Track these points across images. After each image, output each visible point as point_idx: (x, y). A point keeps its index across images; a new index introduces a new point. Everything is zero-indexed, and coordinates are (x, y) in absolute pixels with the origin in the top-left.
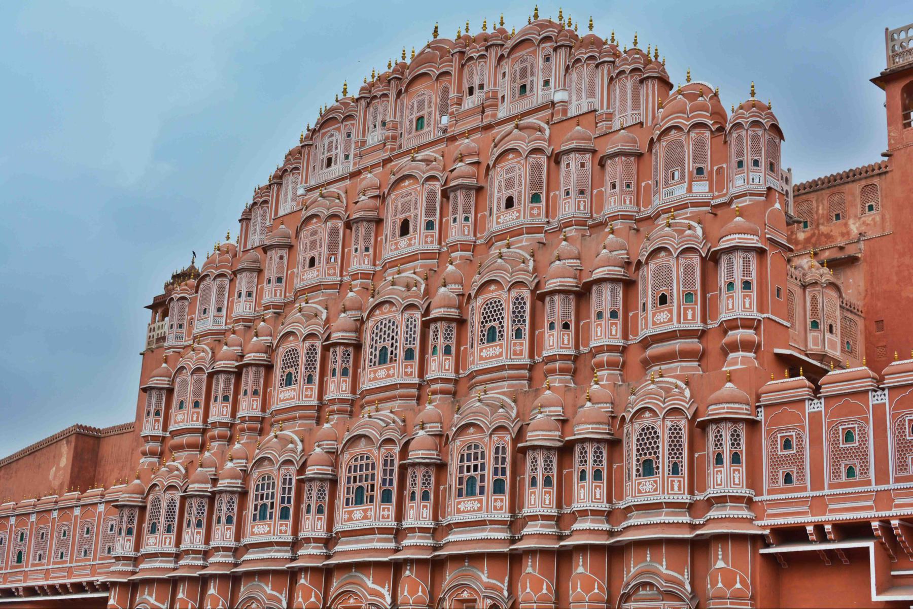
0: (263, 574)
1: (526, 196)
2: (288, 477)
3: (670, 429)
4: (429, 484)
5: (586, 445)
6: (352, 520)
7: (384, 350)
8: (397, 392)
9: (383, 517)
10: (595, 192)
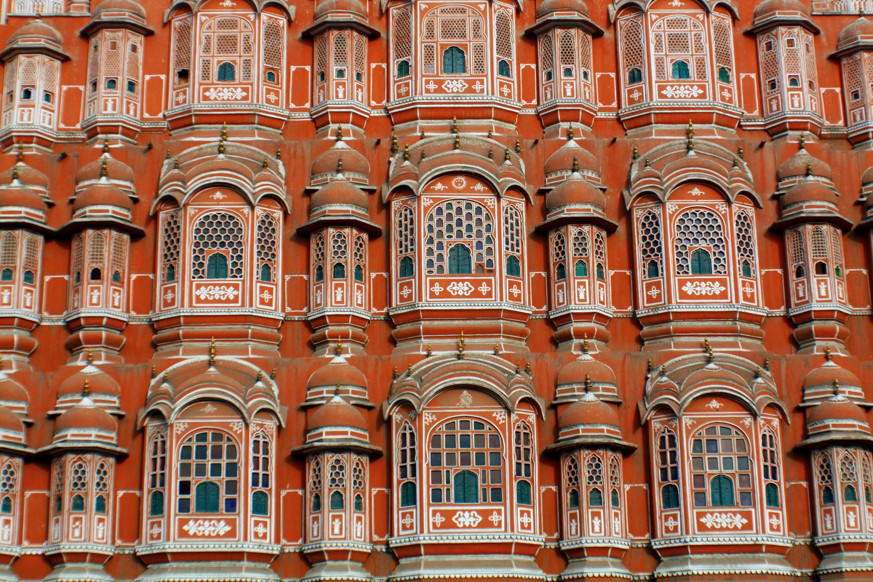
1: (711, 69)
2: (261, 440)
6: (455, 526)
8: (501, 323)
9: (523, 527)
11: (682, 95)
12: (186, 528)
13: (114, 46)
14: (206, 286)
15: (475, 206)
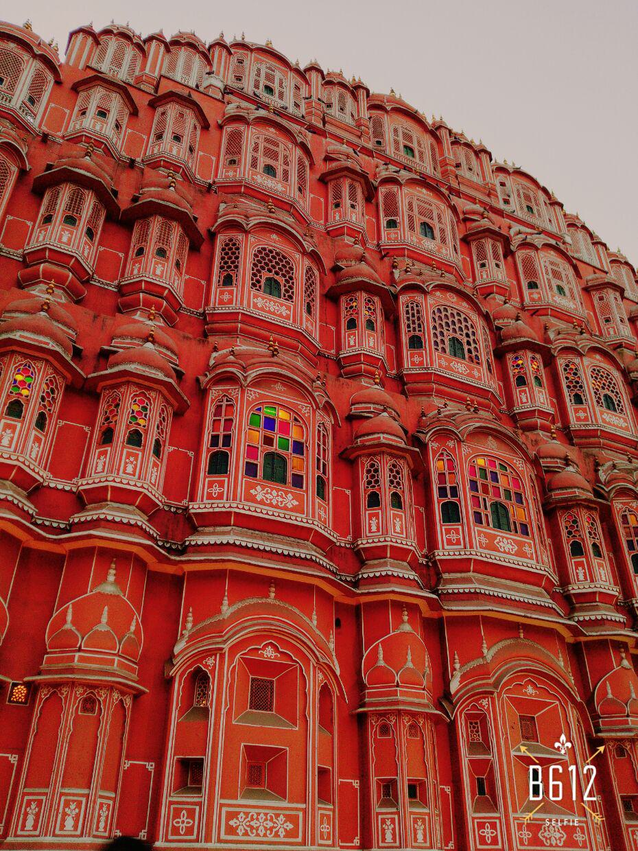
0: (288, 589)
7: (455, 341)
11: (565, 303)
12: (252, 491)
13: (182, 115)
14: (263, 298)
15: (463, 316)
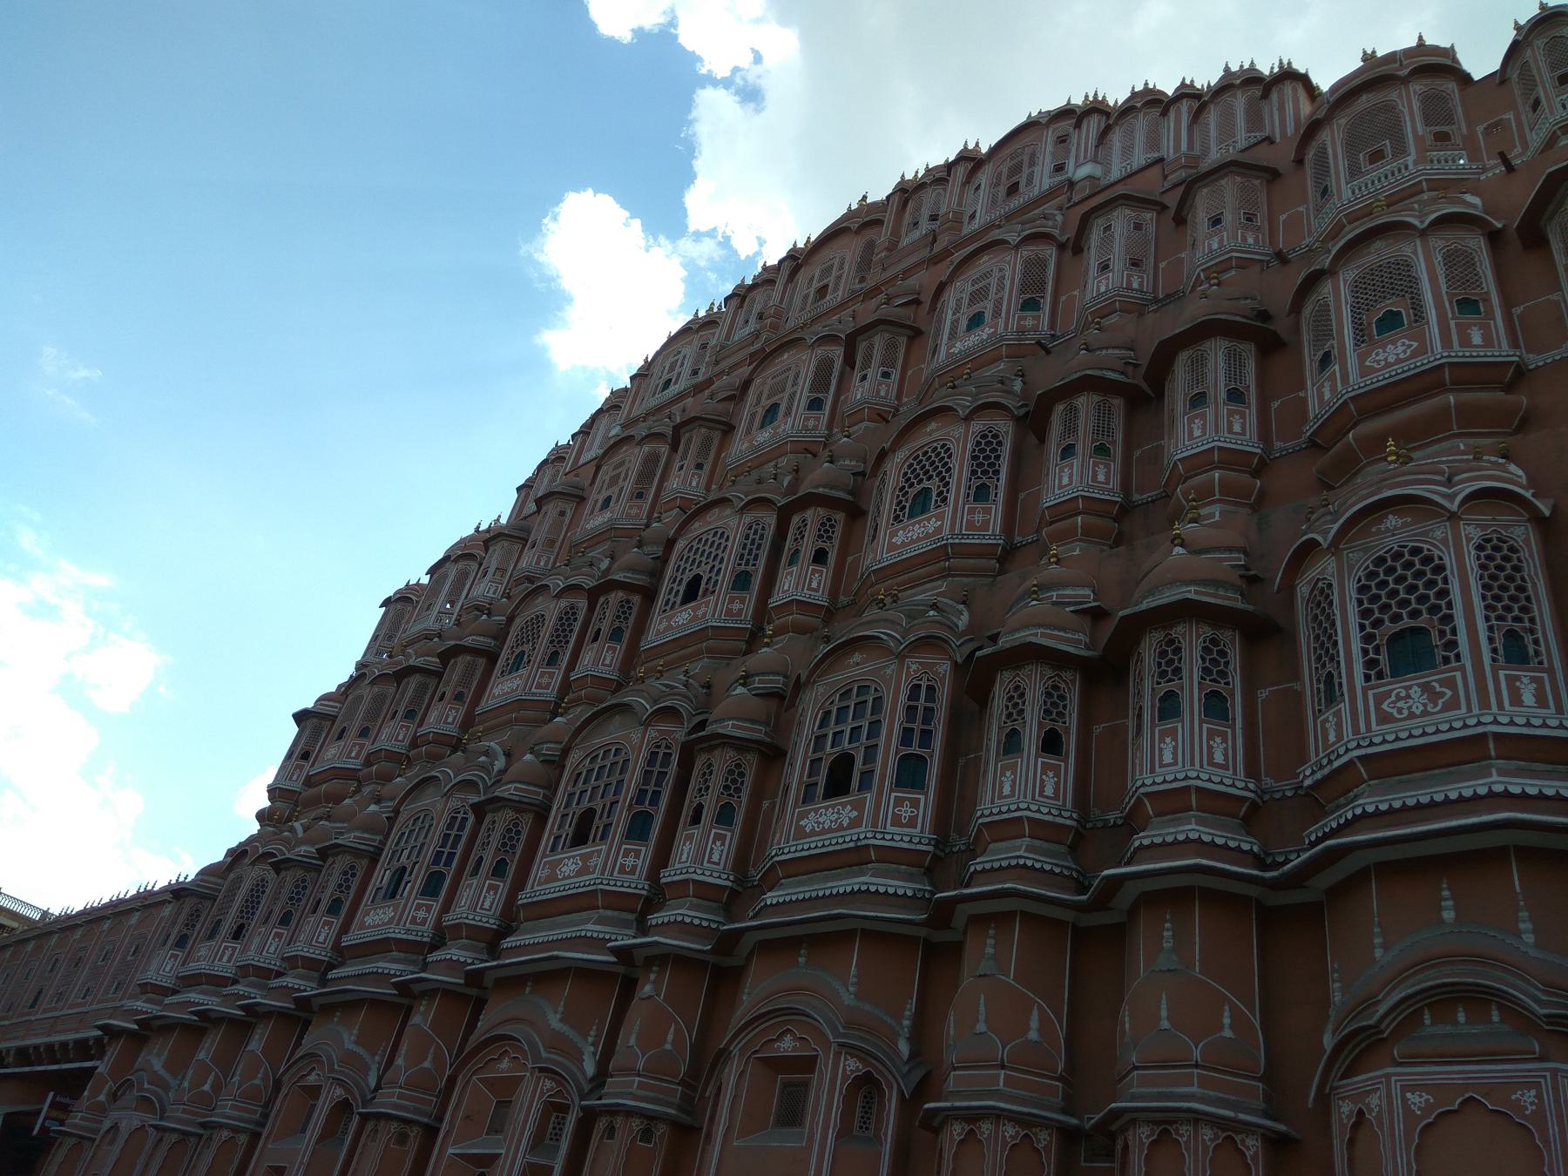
3: (1480, 548)
4: (738, 790)
5: (1178, 631)
9: (622, 870)
10: (1162, 265)
